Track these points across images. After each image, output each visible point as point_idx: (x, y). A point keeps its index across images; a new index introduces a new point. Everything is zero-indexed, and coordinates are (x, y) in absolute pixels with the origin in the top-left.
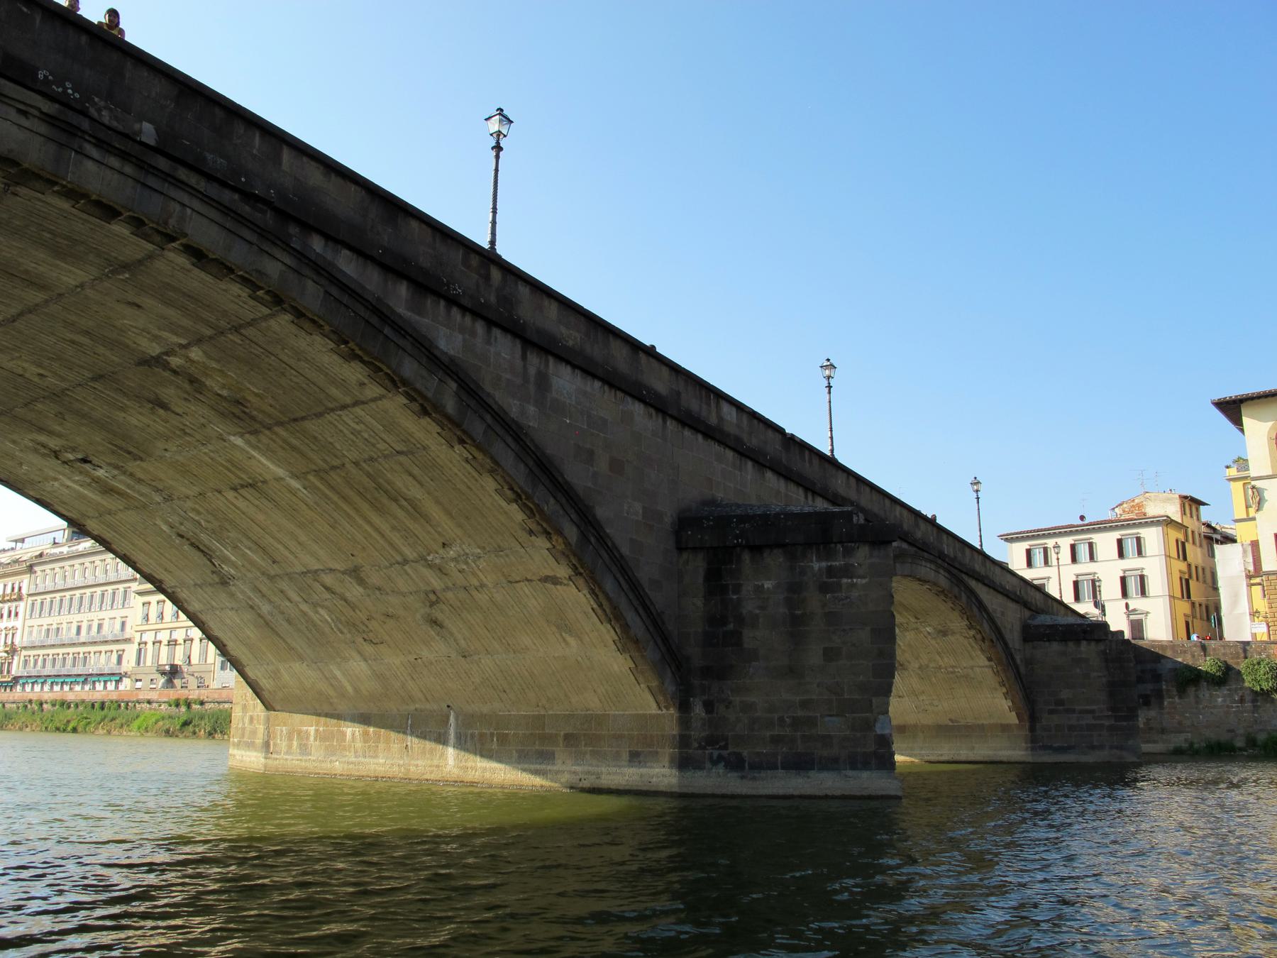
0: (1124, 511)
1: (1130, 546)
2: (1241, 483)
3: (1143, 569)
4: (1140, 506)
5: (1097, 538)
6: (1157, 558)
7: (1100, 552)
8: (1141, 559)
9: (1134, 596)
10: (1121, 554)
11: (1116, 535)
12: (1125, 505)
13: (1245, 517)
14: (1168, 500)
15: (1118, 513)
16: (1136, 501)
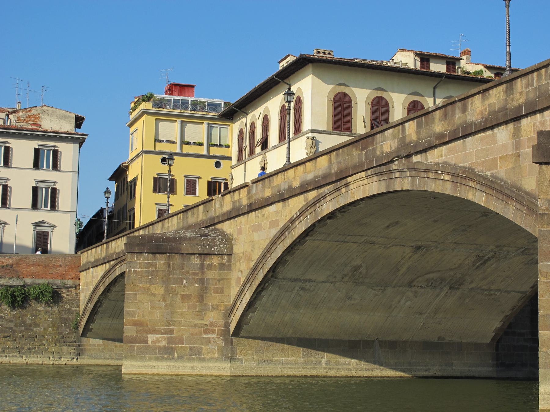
0: (19, 119)
1: (46, 158)
2: (154, 118)
3: (55, 182)
4: (36, 117)
5: (14, 143)
6: (71, 174)
7: (15, 159)
8: (55, 173)
9: (43, 208)
10: (37, 165)
11: (34, 144)
12: (21, 114)
13: (153, 149)
14: (64, 117)
15: (13, 119)
16: (33, 112)
